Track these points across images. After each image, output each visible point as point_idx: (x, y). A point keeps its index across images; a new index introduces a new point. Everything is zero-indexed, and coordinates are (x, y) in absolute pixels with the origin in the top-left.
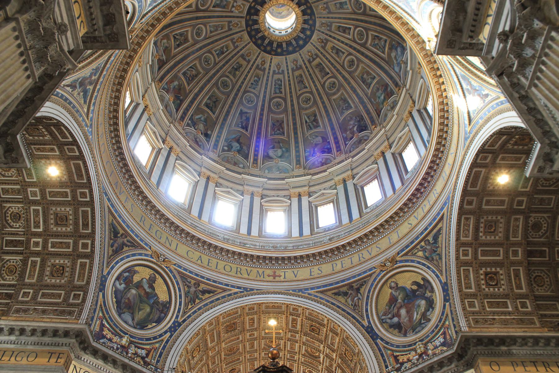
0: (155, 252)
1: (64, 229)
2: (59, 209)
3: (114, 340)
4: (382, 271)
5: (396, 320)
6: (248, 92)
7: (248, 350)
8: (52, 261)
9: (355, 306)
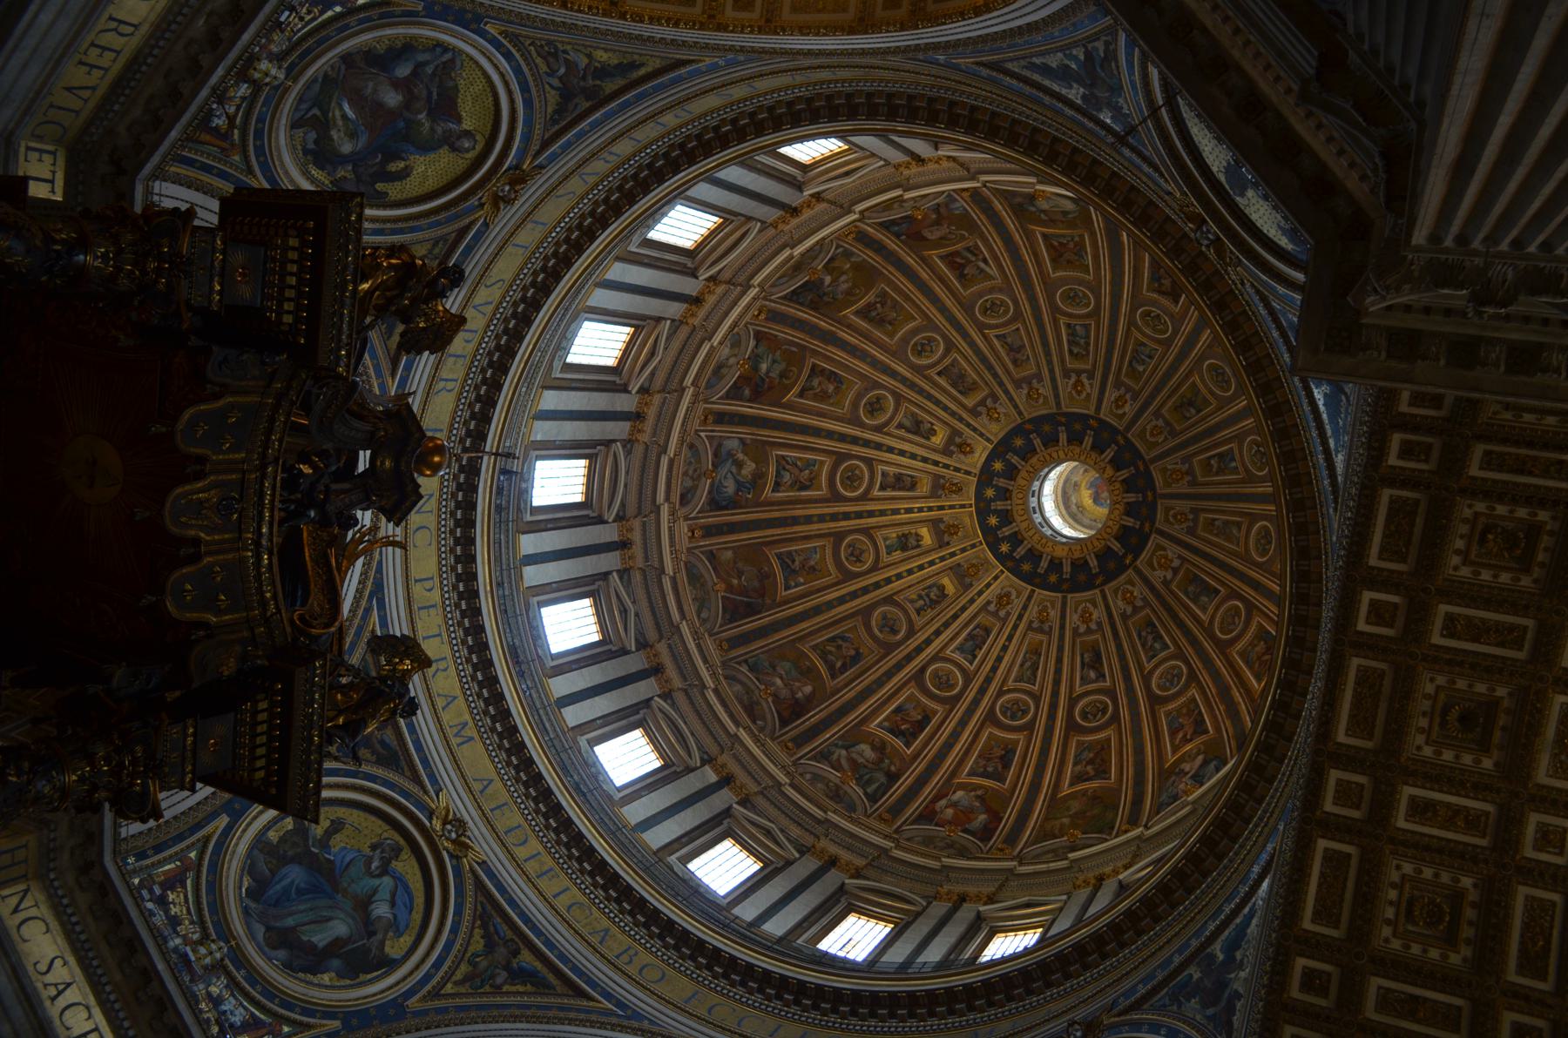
2: (1505, 577)
4: (517, 167)
5: (403, 71)
6: (1159, 342)
9: (552, 54)
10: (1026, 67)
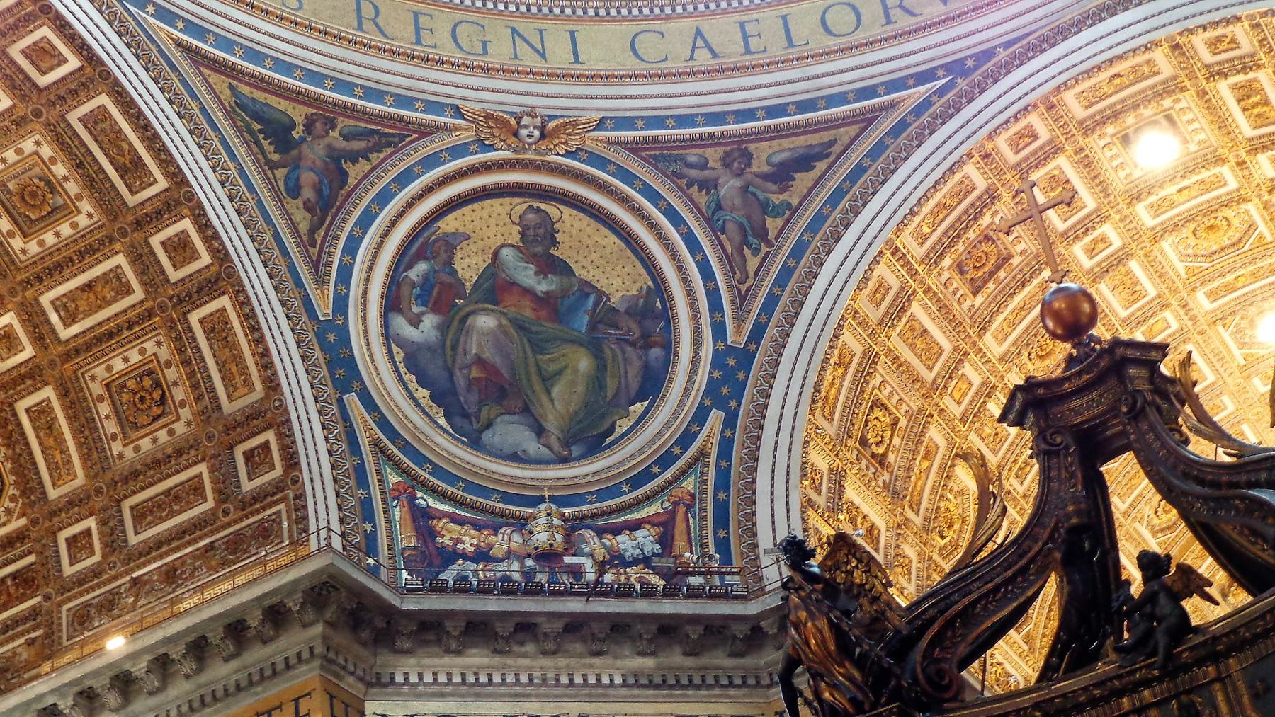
0: (488, 117)
1: (66, 230)
3: (499, 550)
7: (1124, 313)
8: (100, 371)
10: (832, 143)
